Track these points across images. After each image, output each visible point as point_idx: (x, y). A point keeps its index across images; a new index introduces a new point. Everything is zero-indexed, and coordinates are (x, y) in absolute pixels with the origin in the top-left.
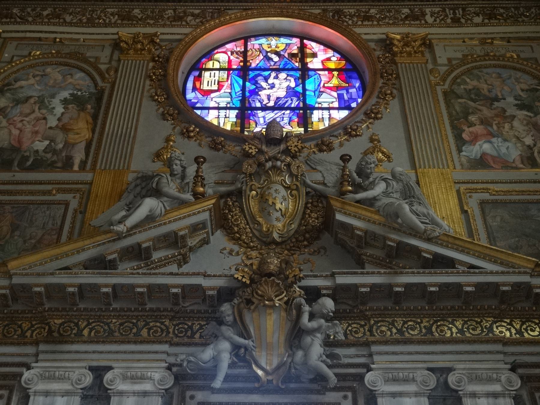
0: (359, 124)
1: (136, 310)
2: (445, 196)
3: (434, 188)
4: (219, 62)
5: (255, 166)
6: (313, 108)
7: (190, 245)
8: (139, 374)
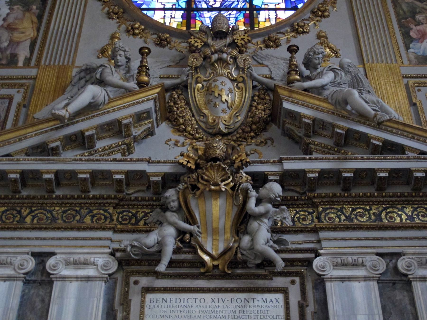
0: (306, 22)
1: (79, 197)
2: (393, 89)
3: (382, 82)
5: (201, 60)
6: (260, 9)
7: (134, 134)
8: (82, 259)
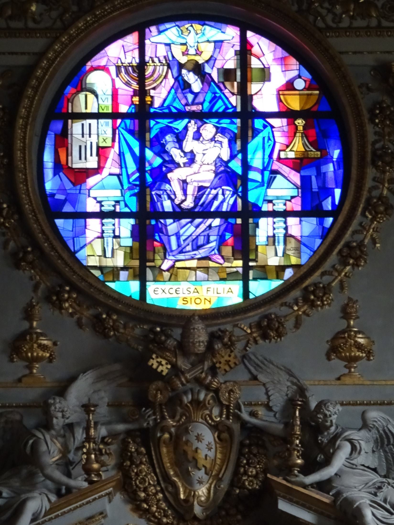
0: (326, 279)
4: (97, 96)
